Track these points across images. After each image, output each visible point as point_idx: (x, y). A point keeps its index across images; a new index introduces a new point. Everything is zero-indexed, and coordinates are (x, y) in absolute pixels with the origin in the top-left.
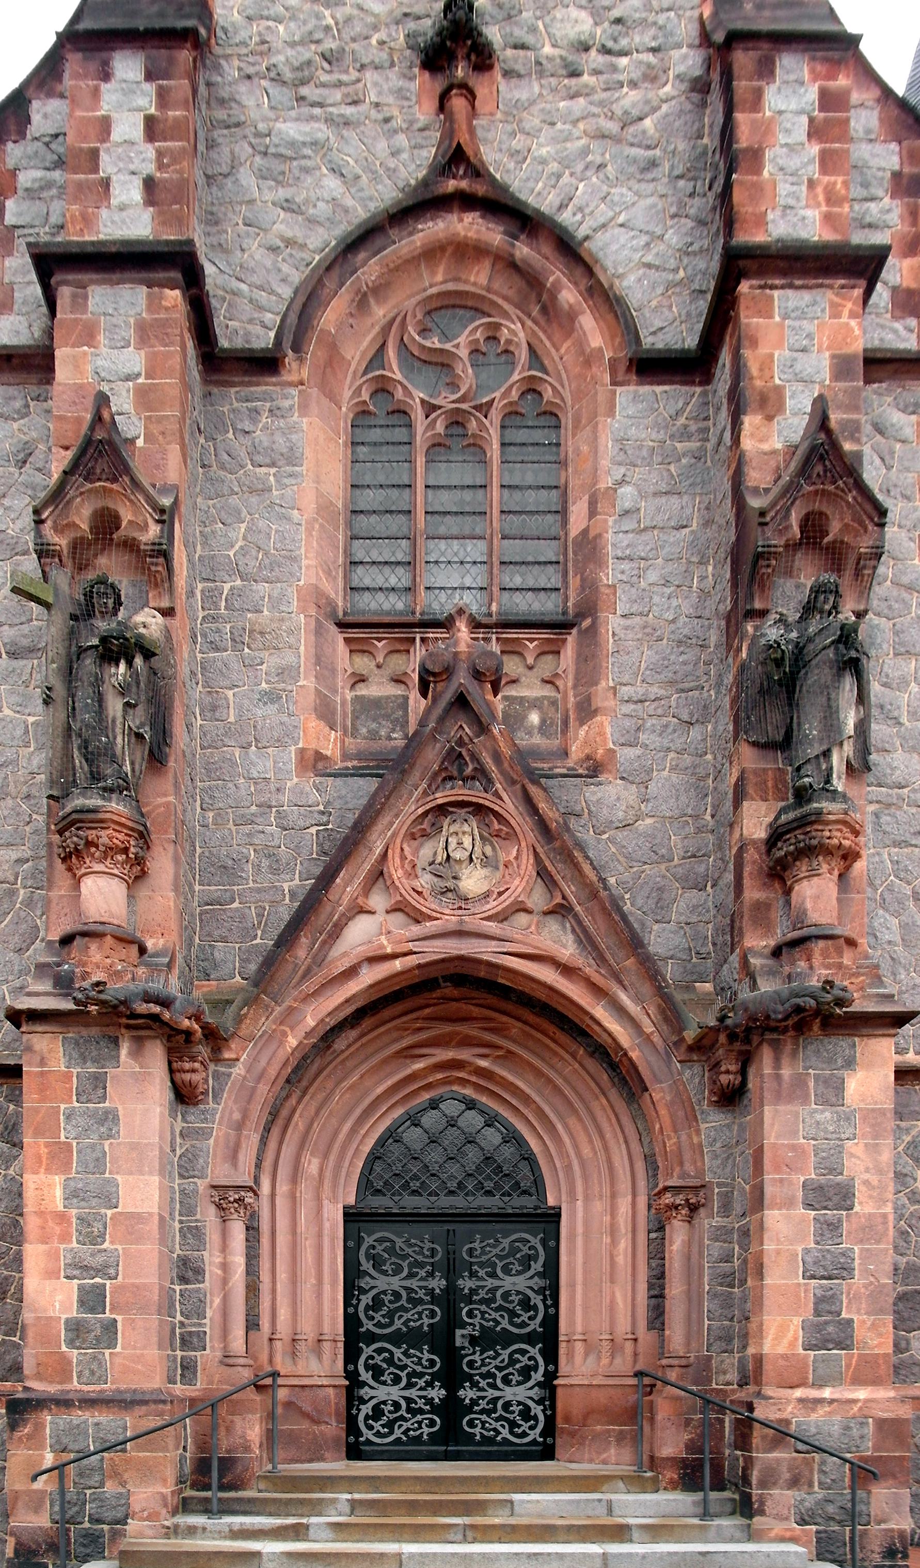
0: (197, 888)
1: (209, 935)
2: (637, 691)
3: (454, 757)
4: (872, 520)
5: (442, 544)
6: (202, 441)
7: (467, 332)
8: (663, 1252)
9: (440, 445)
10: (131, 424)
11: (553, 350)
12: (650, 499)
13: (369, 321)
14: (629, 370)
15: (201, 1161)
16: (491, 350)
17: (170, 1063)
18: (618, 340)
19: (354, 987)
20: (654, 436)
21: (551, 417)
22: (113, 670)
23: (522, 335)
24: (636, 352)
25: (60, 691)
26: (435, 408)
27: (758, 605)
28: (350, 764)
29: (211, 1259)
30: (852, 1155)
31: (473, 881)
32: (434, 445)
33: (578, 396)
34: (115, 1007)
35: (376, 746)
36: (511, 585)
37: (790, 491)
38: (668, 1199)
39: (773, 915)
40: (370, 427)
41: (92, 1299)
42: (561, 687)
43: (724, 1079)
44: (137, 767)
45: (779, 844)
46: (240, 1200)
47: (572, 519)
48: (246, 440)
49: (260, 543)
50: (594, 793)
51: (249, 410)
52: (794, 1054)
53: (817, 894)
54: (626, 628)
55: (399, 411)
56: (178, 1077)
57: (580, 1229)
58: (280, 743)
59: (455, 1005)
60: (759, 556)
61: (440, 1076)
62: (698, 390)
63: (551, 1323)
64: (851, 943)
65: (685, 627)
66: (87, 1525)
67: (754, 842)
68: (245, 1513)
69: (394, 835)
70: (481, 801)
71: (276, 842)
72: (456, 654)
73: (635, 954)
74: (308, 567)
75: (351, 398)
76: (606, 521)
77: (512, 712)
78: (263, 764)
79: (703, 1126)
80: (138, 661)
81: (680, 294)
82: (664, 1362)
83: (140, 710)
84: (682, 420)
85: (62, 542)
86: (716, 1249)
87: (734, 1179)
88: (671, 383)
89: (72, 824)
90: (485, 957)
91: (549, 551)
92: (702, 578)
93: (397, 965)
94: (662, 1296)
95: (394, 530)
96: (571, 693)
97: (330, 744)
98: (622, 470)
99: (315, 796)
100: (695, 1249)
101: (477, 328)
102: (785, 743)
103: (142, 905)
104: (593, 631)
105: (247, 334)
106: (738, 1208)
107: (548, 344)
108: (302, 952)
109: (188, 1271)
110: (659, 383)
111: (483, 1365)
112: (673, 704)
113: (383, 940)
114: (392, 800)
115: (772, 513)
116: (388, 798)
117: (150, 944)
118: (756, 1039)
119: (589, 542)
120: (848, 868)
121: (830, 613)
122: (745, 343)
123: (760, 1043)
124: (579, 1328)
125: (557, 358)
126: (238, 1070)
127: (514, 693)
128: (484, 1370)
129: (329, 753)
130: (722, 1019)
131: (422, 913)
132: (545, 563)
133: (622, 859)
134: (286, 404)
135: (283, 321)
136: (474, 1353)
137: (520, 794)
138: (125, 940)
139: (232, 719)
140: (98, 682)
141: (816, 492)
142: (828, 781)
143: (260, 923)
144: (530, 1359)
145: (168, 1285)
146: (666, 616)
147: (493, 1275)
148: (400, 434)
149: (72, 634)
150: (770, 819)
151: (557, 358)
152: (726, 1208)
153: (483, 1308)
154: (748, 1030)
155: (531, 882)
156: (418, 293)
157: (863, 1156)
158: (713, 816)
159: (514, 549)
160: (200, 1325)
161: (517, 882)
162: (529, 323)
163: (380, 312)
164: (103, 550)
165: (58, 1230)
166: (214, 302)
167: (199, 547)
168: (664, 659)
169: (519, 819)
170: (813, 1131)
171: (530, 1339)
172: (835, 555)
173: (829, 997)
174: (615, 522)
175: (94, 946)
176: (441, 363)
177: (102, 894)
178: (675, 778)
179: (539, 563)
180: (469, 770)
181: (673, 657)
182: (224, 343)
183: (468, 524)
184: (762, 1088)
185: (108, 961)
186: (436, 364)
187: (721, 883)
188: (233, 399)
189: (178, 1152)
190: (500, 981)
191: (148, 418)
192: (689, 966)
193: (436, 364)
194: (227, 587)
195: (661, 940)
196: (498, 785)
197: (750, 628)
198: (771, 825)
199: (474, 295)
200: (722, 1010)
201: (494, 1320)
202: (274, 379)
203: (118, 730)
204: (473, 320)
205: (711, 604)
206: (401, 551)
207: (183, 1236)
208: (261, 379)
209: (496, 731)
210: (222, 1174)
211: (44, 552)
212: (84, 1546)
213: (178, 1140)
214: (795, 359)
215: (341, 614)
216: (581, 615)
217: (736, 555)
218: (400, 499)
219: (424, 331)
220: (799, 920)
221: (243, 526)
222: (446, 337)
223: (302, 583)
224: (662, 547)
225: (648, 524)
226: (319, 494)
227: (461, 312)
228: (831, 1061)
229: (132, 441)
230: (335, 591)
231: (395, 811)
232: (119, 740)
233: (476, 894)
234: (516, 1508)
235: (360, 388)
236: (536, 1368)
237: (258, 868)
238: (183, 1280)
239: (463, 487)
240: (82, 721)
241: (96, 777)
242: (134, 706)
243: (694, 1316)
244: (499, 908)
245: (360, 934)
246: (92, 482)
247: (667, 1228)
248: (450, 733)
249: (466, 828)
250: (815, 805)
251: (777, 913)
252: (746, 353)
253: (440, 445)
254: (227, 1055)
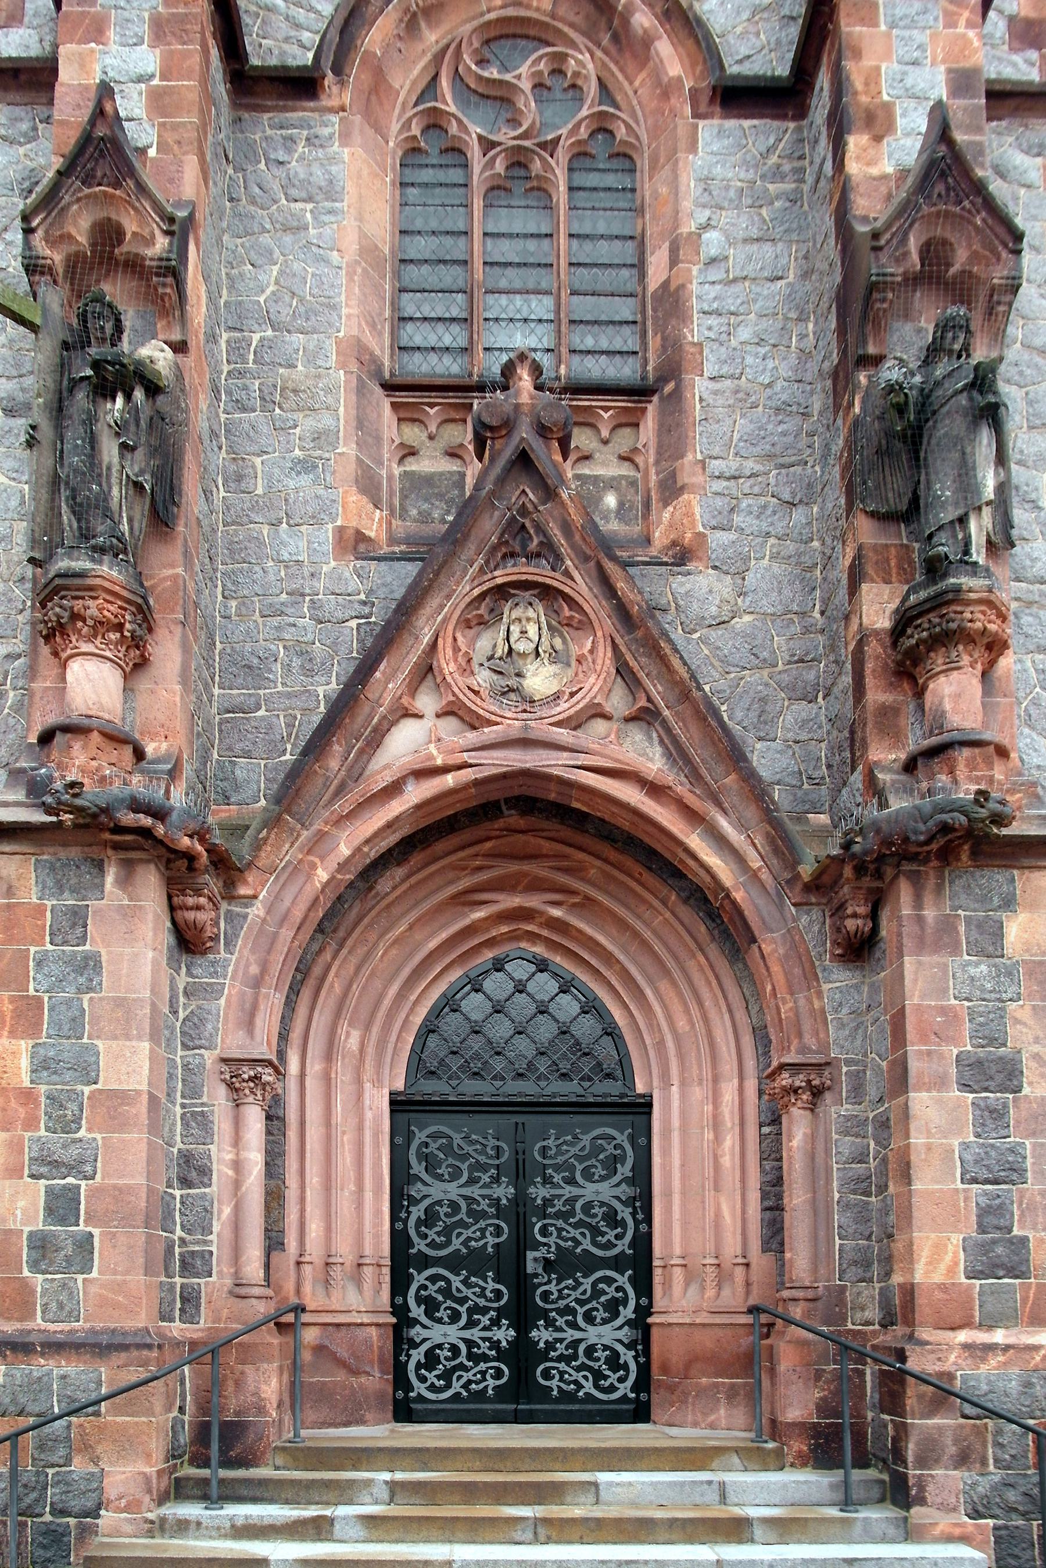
0: (216, 691)
1: (230, 749)
2: (731, 465)
3: (516, 529)
4: (1006, 246)
5: (504, 300)
6: (230, 171)
7: (529, 62)
8: (779, 1151)
9: (499, 187)
10: (141, 132)
11: (626, 84)
12: (740, 246)
13: (420, 47)
14: (712, 101)
15: (209, 1026)
16: (558, 84)
17: (170, 897)
18: (699, 68)
19: (396, 807)
20: (742, 175)
21: (624, 158)
22: (109, 406)
23: (590, 66)
24: (720, 78)
25: (46, 432)
26: (493, 145)
27: (871, 350)
28: (397, 549)
29: (220, 1155)
30: (1017, 1021)
31: (540, 679)
32: (492, 188)
33: (655, 133)
34: (95, 816)
35: (427, 530)
36: (582, 347)
37: (906, 211)
38: (785, 1079)
39: (902, 721)
40: (420, 166)
41: (62, 1206)
42: (641, 465)
43: (851, 924)
44: (136, 525)
45: (909, 631)
46: (255, 1079)
47: (650, 271)
48: (280, 172)
49: (294, 288)
50: (682, 584)
51: (284, 138)
52: (939, 889)
53: (955, 693)
54: (715, 393)
55: (453, 149)
56: (180, 915)
57: (676, 1123)
58: (315, 521)
59: (522, 837)
60: (873, 287)
61: (504, 929)
62: (792, 125)
63: (643, 1243)
64: (1002, 752)
65: (783, 392)
66: (48, 1518)
67: (876, 633)
68: (255, 1500)
69: (446, 620)
70: (548, 581)
71: (310, 637)
72: (517, 406)
73: (737, 769)
74: (349, 317)
75: (400, 132)
76: (690, 270)
77: (584, 493)
78: (295, 544)
79: (825, 987)
80: (139, 394)
81: (767, 20)
82: (786, 1294)
83: (140, 453)
84: (774, 159)
85: (57, 257)
86: (846, 1145)
87: (865, 1055)
88: (761, 116)
89: (56, 591)
90: (556, 772)
91: (625, 309)
92: (802, 337)
93: (449, 780)
94: (779, 1208)
95: (448, 282)
96: (653, 471)
97: (374, 525)
98: (707, 213)
99: (354, 583)
100: (820, 1147)
101: (541, 58)
102: (910, 512)
103: (142, 700)
104: (677, 395)
105: (283, 53)
106: (872, 1092)
107: (620, 76)
108: (334, 763)
110: (746, 118)
111: (561, 1297)
112: (772, 481)
113: (433, 749)
114: (442, 578)
115: (887, 236)
116: (437, 574)
117: (150, 749)
118: (889, 872)
119: (670, 295)
120: (992, 663)
121: (959, 357)
122: (847, 53)
123: (896, 877)
124: (678, 1251)
125: (630, 93)
126: (256, 911)
127: (587, 472)
128: (562, 1303)
129: (372, 534)
130: (847, 846)
131: (479, 717)
132: (621, 323)
133: (717, 664)
134: (326, 131)
135: (322, 40)
136: (549, 1282)
137: (594, 573)
138: (115, 738)
139: (260, 491)
140: (91, 420)
141: (938, 214)
142: (967, 552)
143: (290, 735)
144: (618, 1289)
145: (162, 1187)
146: (761, 379)
147: (571, 1181)
148: (455, 175)
149: (63, 366)
150: (893, 606)
151: (630, 93)
152: (857, 1092)
153: (560, 1223)
154: (881, 858)
155: (610, 680)
156: (474, 18)
157: (1030, 1022)
158: (822, 613)
159: (583, 307)
160: (205, 1242)
161: (592, 680)
162: (599, 53)
163: (432, 38)
164: (107, 275)
165: (22, 1112)
166: (246, 19)
167: (225, 292)
168: (760, 429)
169: (594, 602)
170: (966, 990)
171: (617, 1263)
172: (960, 290)
173: (983, 813)
174: (700, 271)
175: (77, 746)
176: (499, 97)
177: (92, 682)
178: (776, 568)
179: (613, 323)
180: (534, 545)
181: (770, 427)
182: (255, 61)
183: (532, 277)
184: (900, 935)
185: (94, 763)
186: (495, 98)
187: (836, 690)
188: (265, 126)
189: (182, 1015)
190: (576, 805)
191: (162, 125)
192: (800, 793)
193: (495, 98)
194: (256, 338)
195: (767, 759)
196: (569, 563)
197: (862, 378)
198: (897, 611)
199: (537, 23)
200: (846, 834)
201: (574, 1239)
202: (312, 104)
203: (114, 480)
204: (536, 50)
205: (813, 367)
206: (456, 305)
207: (186, 1125)
208: (298, 104)
209: (565, 495)
210: (232, 1042)
211: (33, 267)
212: (44, 1547)
213: (182, 999)
214: (905, 73)
215: (387, 375)
216: (662, 379)
217: (842, 300)
218: (456, 248)
219: (481, 62)
220: (938, 724)
221: (275, 269)
222: (505, 68)
223: (341, 334)
224: (755, 301)
225: (738, 273)
226: (362, 235)
227: (523, 43)
228: (985, 899)
229: (142, 151)
230: (381, 347)
231: (446, 591)
232: (115, 492)
233: (544, 695)
234: (602, 1493)
235: (409, 120)
236: (625, 1302)
237: (288, 668)
238: (185, 1182)
239: (526, 236)
240: (70, 465)
241: (85, 535)
242: (133, 449)
243: (822, 1233)
244: (572, 711)
245: (406, 743)
246: (90, 186)
247: (785, 1119)
248: (514, 484)
249: (530, 613)
250: (952, 580)
251: (908, 719)
252: (848, 64)
253: (499, 187)
254: (243, 891)
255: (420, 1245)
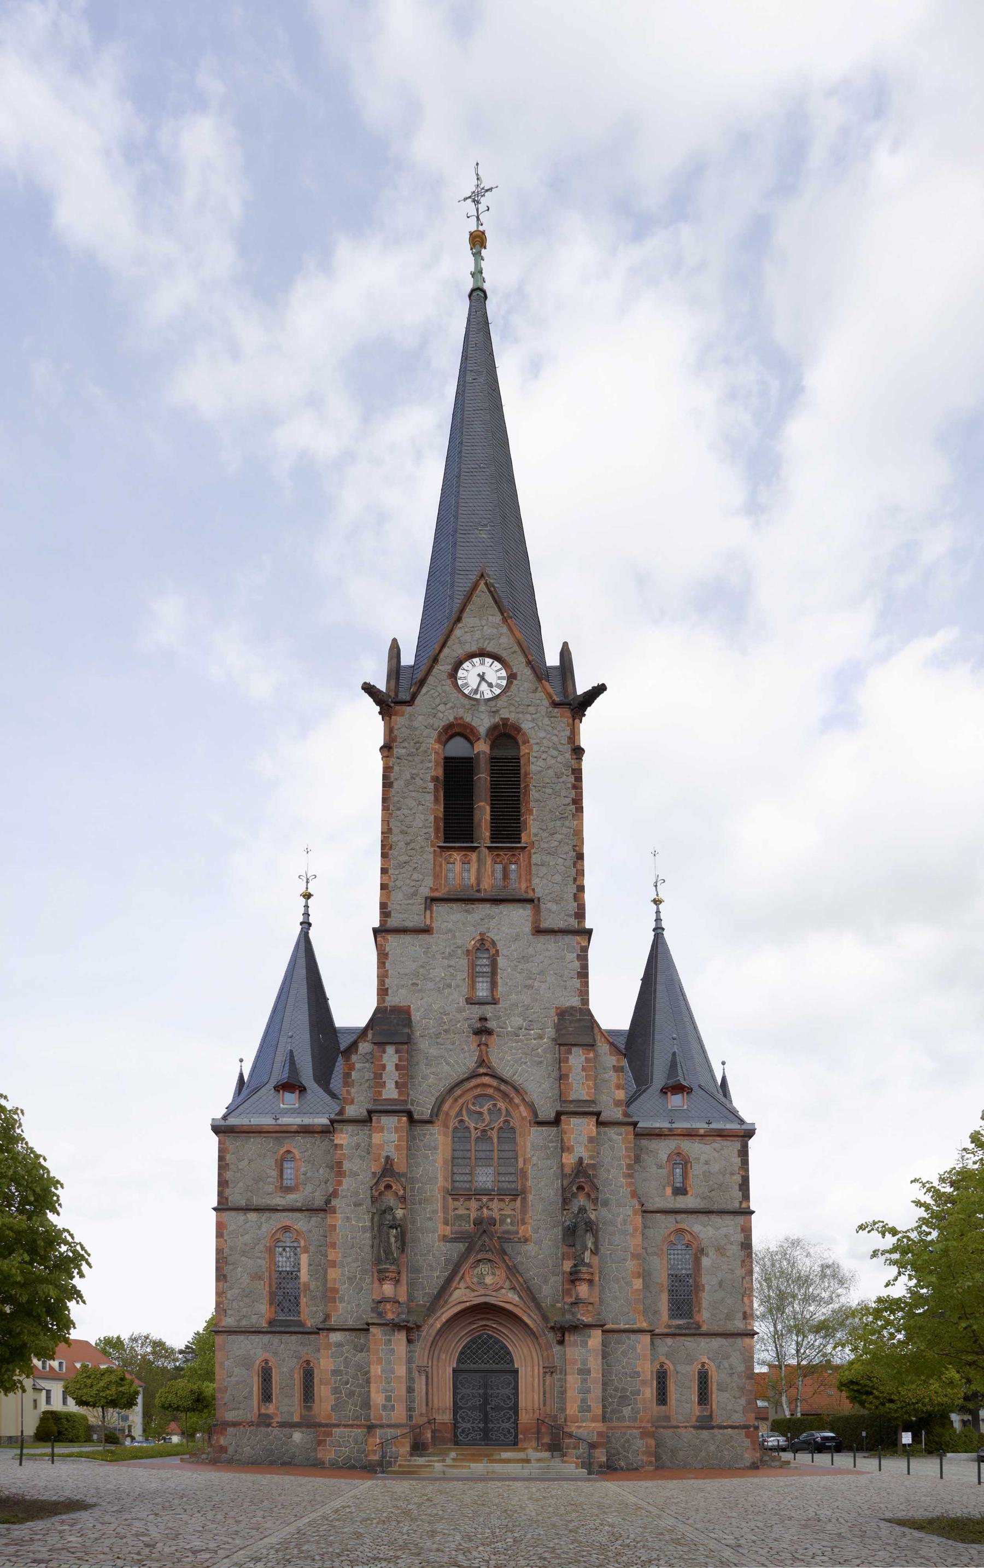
31: (489, 1280)
93: (468, 1304)
109: (410, 1390)
140: (388, 1234)
171: (510, 1408)
238: (409, 1392)
255: (460, 1404)
